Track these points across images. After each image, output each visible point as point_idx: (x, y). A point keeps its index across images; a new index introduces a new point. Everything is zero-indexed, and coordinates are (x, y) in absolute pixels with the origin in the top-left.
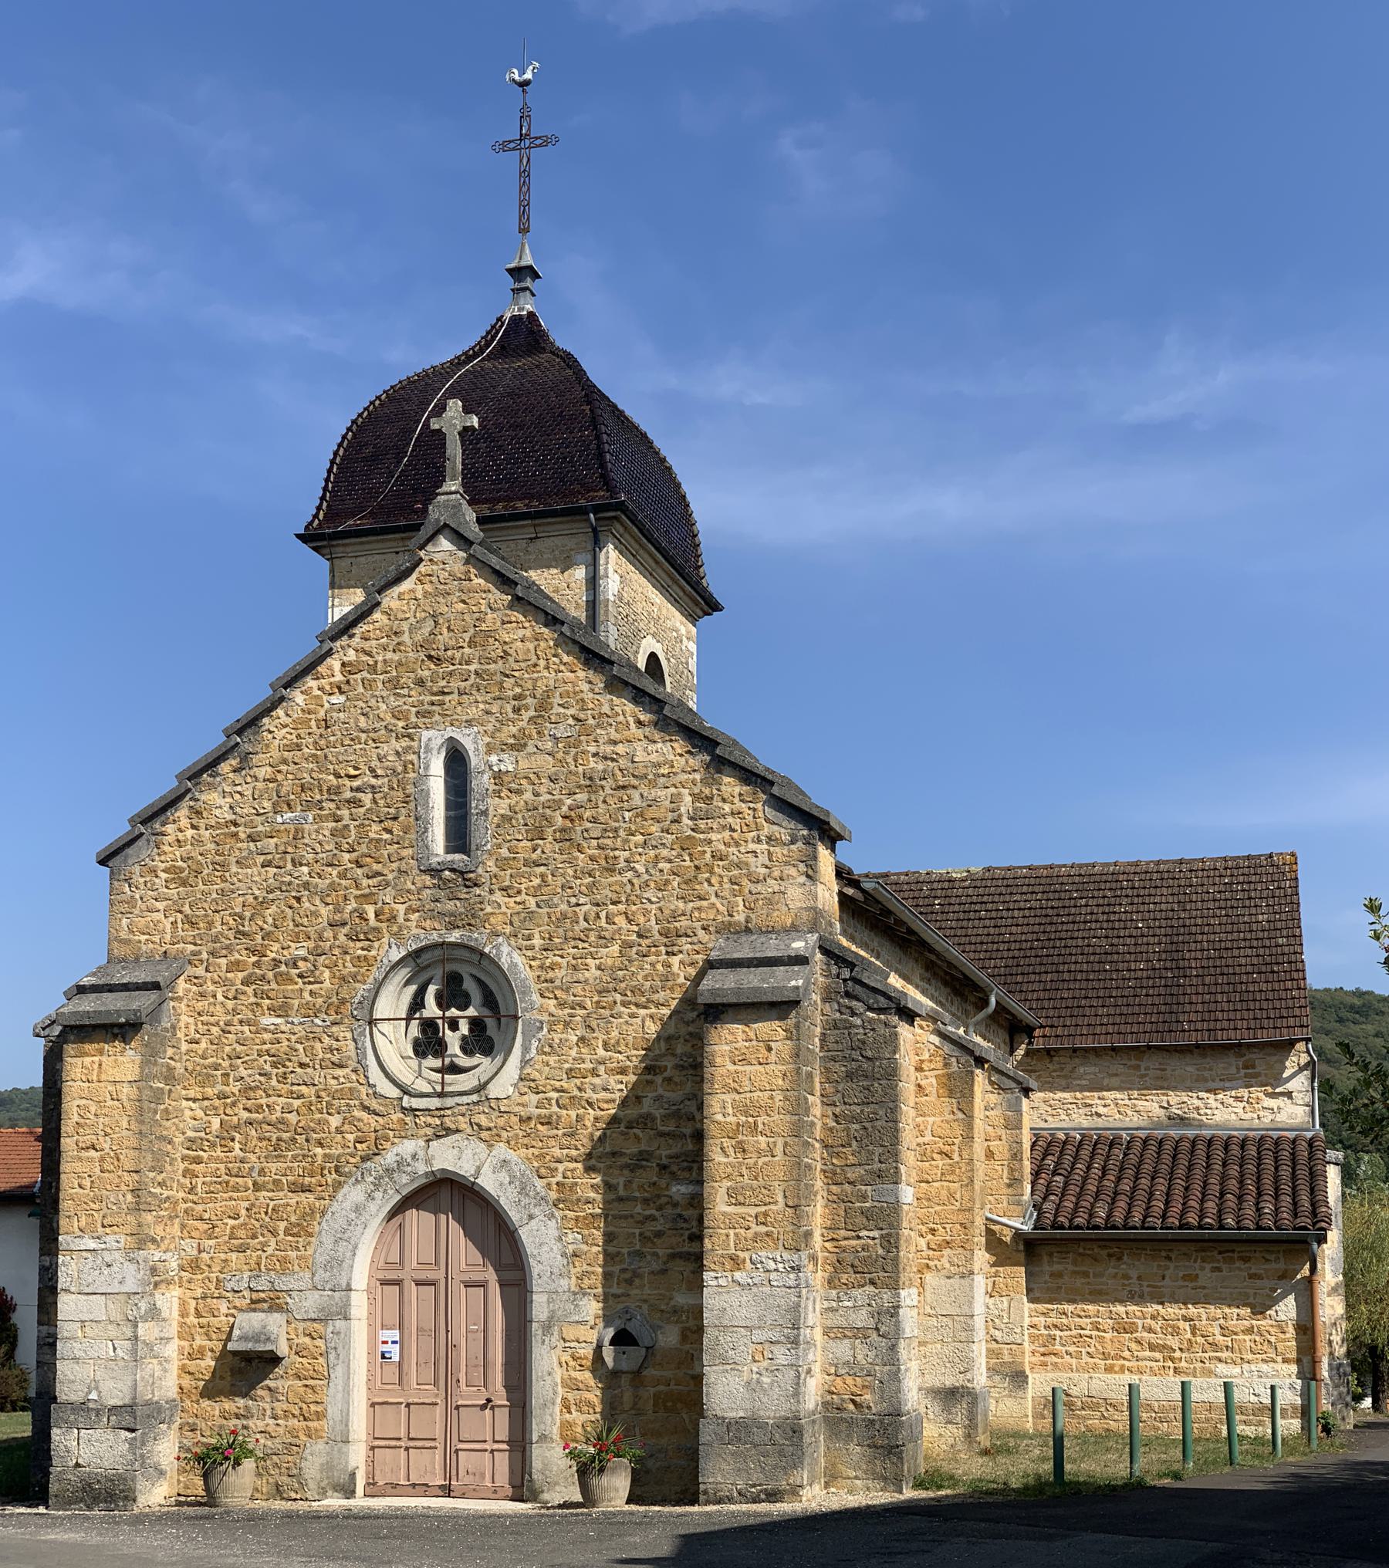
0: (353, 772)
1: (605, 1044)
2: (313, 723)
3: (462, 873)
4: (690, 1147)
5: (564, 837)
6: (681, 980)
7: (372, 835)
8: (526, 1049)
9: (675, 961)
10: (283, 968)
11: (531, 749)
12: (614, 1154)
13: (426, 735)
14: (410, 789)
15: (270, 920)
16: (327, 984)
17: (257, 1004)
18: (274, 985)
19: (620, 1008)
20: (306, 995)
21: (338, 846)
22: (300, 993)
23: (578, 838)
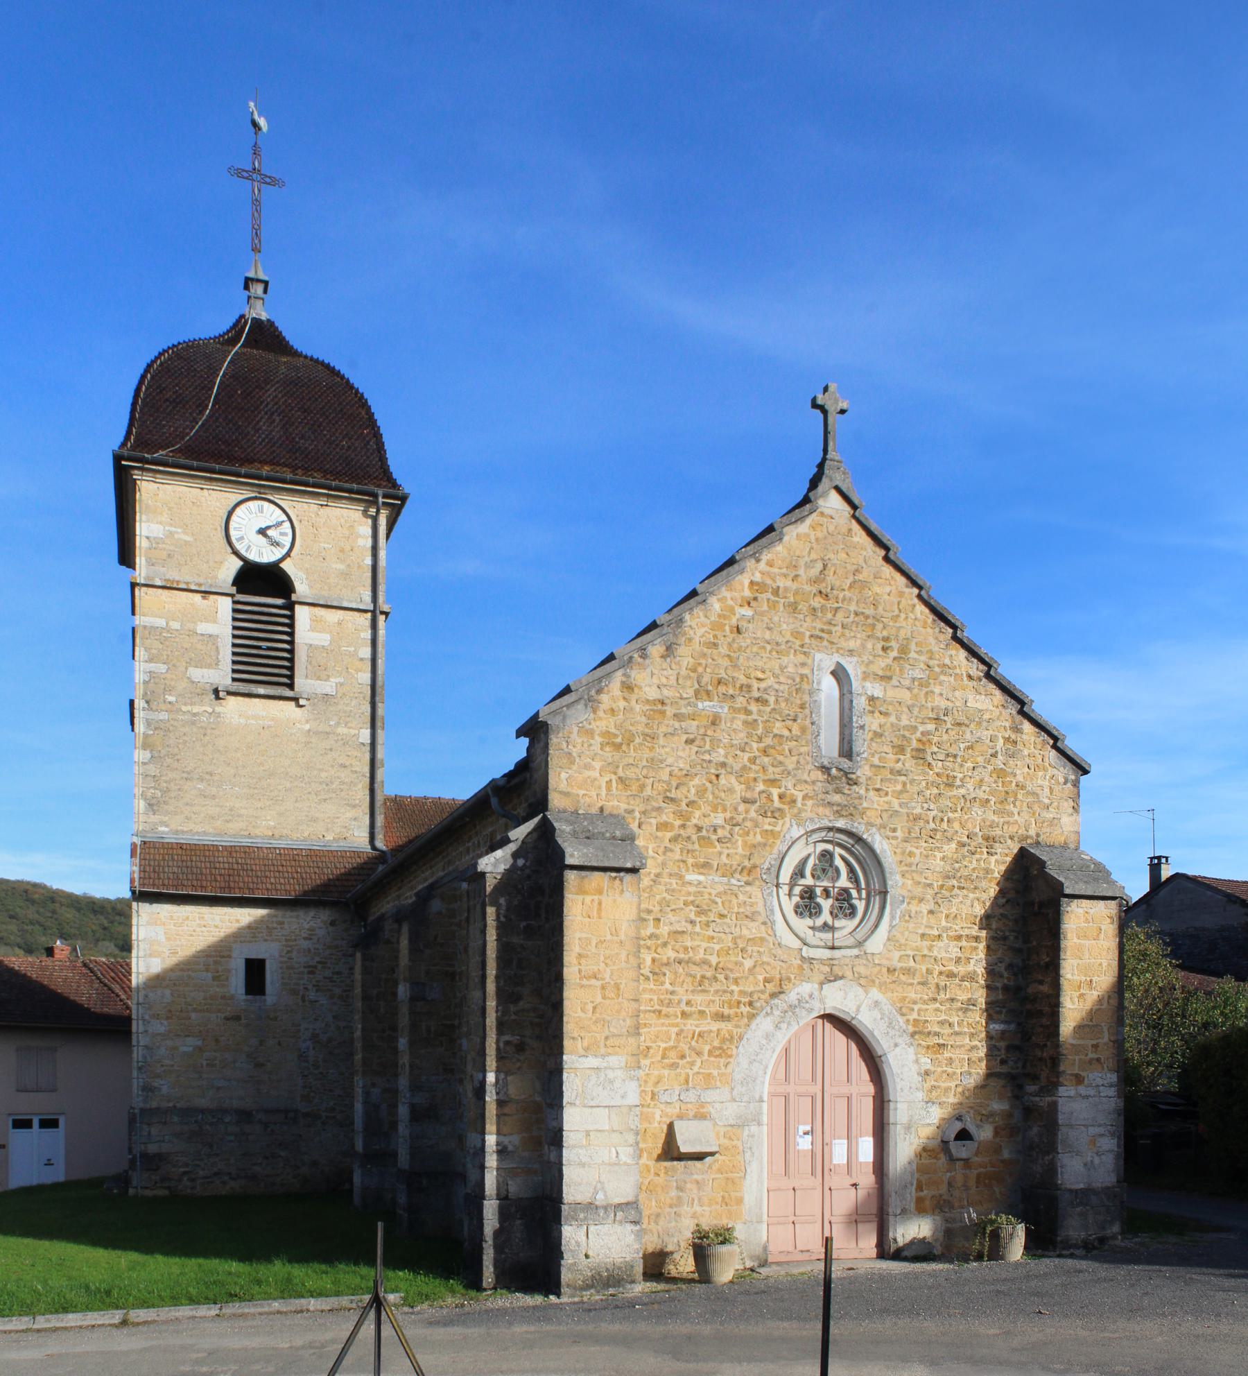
0: (760, 675)
1: (947, 916)
2: (727, 628)
3: (846, 774)
5: (919, 754)
6: (996, 875)
7: (776, 731)
8: (893, 917)
9: (993, 859)
10: (704, 833)
11: (894, 682)
12: (952, 1000)
13: (818, 656)
14: (806, 698)
15: (693, 791)
16: (740, 850)
17: (684, 861)
18: (696, 846)
20: (724, 857)
21: (749, 735)
23: (929, 759)
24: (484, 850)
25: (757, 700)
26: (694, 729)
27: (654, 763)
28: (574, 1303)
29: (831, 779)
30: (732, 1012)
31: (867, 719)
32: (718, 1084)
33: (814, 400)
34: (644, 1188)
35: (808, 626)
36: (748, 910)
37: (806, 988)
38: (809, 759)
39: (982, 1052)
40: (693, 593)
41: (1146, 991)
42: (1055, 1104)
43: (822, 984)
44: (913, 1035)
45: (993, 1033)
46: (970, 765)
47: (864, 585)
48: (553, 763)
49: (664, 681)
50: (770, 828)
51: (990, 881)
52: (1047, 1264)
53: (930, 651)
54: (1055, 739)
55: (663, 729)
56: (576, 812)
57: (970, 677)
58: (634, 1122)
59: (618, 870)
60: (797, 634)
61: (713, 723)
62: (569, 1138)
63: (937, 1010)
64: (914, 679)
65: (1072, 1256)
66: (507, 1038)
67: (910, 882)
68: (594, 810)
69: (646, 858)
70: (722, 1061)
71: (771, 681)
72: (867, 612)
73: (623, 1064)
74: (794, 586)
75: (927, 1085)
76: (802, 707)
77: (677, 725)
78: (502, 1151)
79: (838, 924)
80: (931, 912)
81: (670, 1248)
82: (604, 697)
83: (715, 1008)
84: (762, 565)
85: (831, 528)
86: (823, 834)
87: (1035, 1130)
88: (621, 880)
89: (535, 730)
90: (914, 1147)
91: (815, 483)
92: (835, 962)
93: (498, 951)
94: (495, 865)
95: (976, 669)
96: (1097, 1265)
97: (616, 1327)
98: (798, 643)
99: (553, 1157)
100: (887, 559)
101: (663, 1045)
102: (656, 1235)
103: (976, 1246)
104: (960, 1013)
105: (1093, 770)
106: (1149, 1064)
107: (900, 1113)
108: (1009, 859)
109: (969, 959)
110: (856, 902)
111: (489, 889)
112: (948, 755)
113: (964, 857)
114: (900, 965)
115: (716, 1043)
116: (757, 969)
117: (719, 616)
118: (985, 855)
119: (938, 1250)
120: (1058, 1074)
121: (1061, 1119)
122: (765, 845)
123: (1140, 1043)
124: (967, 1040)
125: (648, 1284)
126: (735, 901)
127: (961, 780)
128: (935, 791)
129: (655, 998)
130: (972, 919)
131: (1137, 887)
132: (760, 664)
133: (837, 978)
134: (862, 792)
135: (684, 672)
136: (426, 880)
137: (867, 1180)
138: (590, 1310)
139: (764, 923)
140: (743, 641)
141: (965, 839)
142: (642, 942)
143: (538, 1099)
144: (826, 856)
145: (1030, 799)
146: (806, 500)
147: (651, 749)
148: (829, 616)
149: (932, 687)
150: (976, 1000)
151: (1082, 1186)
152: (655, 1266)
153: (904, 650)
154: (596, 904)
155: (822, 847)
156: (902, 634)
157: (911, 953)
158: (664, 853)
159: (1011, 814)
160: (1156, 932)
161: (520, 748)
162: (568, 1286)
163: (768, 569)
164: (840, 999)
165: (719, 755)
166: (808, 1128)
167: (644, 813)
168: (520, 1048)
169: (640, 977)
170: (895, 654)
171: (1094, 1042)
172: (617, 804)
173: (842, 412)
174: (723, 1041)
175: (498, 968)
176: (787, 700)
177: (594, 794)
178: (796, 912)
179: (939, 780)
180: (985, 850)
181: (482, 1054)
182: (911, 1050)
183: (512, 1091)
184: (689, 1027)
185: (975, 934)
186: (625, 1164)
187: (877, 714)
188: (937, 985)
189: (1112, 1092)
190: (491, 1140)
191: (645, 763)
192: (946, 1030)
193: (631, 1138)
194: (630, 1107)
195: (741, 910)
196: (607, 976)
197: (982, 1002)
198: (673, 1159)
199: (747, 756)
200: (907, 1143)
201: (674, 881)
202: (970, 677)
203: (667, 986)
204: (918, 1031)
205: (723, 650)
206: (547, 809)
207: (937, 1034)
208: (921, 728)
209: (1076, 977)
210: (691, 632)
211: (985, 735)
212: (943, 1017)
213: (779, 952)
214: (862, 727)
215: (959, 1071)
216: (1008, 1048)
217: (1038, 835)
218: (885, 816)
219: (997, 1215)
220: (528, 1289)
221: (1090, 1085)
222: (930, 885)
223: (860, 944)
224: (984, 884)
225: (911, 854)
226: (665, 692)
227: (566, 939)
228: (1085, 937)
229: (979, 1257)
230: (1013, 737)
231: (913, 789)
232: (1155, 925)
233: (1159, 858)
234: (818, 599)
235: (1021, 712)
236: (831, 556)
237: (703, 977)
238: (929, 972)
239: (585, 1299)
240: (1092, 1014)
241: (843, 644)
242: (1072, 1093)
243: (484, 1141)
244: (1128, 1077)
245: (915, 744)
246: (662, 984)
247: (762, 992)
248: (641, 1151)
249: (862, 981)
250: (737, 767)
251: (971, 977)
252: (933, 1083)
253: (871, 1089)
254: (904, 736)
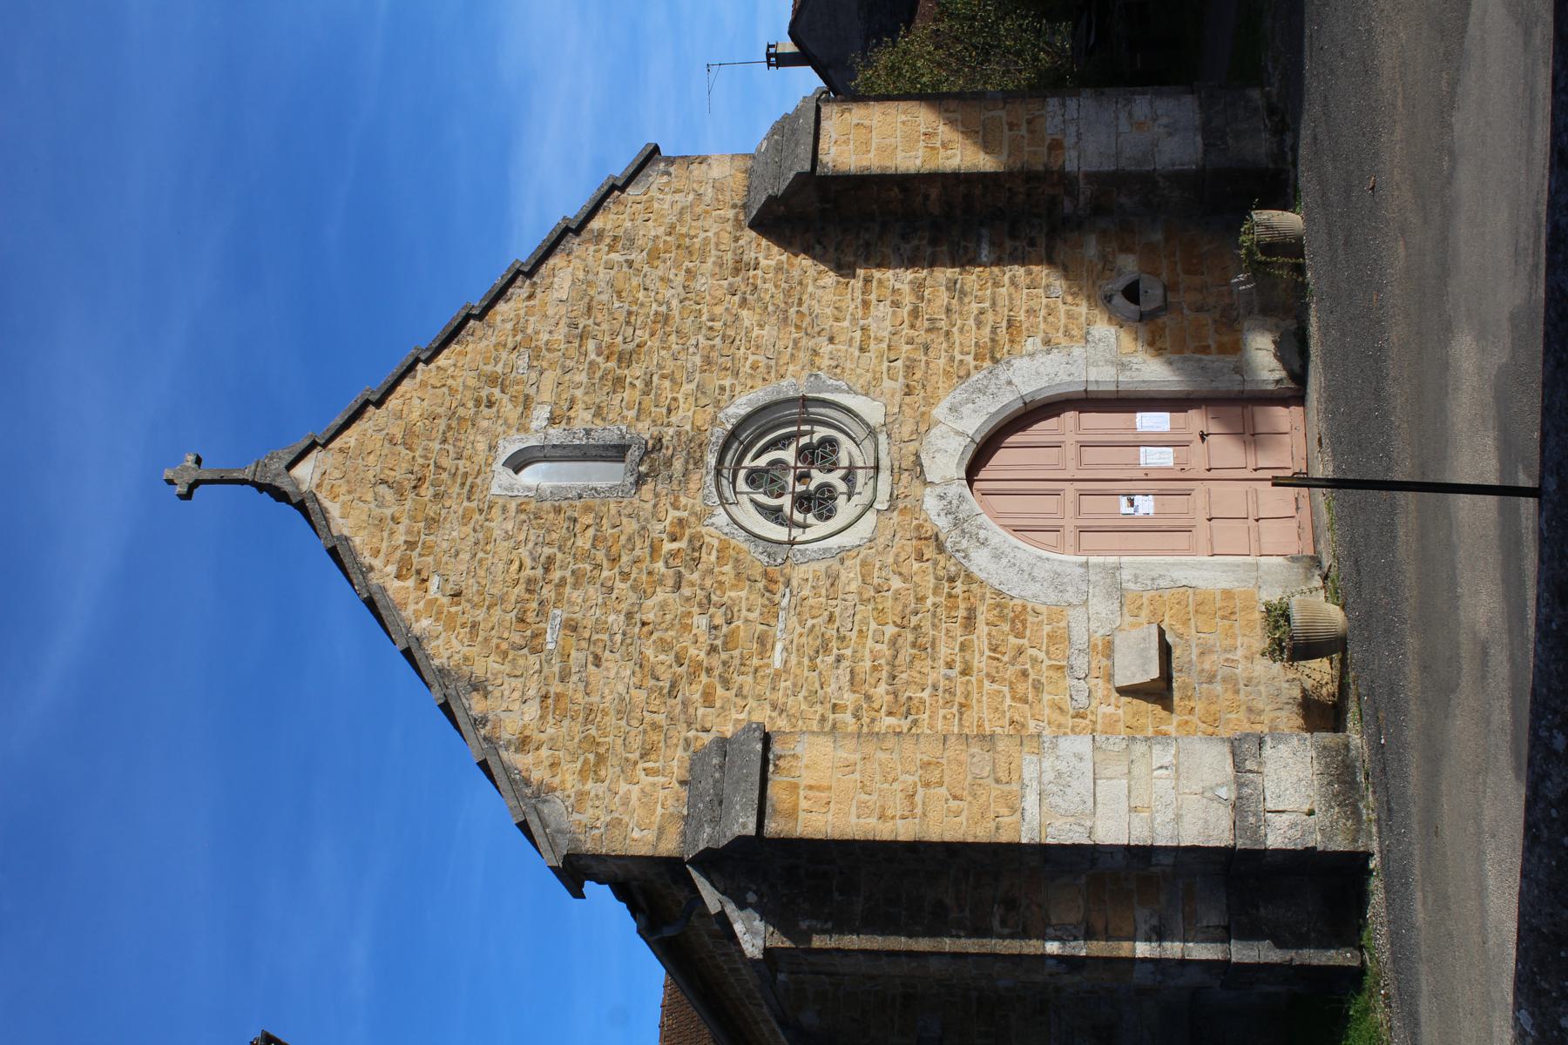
0: (516, 566)
1: (837, 319)
2: (453, 609)
3: (647, 453)
4: (945, 248)
5: (625, 359)
6: (784, 258)
7: (588, 546)
8: (838, 389)
9: (763, 263)
10: (718, 642)
11: (532, 391)
12: (948, 310)
13: (495, 490)
14: (547, 505)
15: (662, 657)
16: (743, 594)
17: (756, 671)
18: (736, 653)
19: (804, 309)
20: (752, 616)
21: (592, 581)
22: (748, 622)
23: (631, 346)
24: (734, 948)
25: (547, 570)
26: (581, 655)
28: (1380, 832)
29: (653, 473)
30: (962, 606)
31: (578, 425)
32: (1063, 624)
33: (183, 497)
34: (1211, 730)
35: (456, 503)
36: (824, 583)
37: (931, 504)
38: (626, 501)
39: (1019, 271)
40: (407, 654)
41: (939, 65)
42: (1088, 175)
43: (926, 483)
44: (995, 361)
45: (993, 257)
46: (641, 295)
47: (409, 432)
48: (619, 848)
49: (516, 695)
50: (714, 553)
51: (792, 265)
52: (1306, 180)
53: (496, 346)
54: (613, 188)
55: (579, 697)
56: (686, 819)
57: (531, 297)
58: (1117, 744)
59: (765, 762)
60: (466, 518)
61: (574, 629)
62: (1139, 835)
63: (961, 330)
64: (530, 367)
65: (1294, 149)
66: (996, 923)
67: (791, 368)
68: (684, 793)
69: (750, 723)
70: (1030, 619)
71: (524, 552)
72: (442, 428)
73: (1035, 758)
74: (405, 521)
75: (1064, 342)
76: (558, 510)
77: (575, 678)
78: (1159, 934)
79: (845, 462)
80: (831, 340)
81: (1297, 693)
82: (536, 776)
83: (957, 630)
84: (377, 563)
85: (337, 474)
86: (724, 482)
87: (1123, 200)
88: (779, 757)
89: (575, 871)
90: (1147, 357)
91: (280, 495)
92: (896, 464)
93: (873, 933)
94: (755, 934)
95: (520, 290)
96: (1305, 117)
97: (1414, 773)
98: (476, 516)
99: (1168, 860)
100: (379, 404)
101: (1008, 701)
102: (1278, 713)
103: (1284, 273)
104: (966, 300)
105: (653, 141)
106: (1036, 59)
107: (1102, 377)
108: (764, 242)
109: (894, 291)
110: (816, 438)
111: (788, 944)
112: (628, 323)
113: (760, 299)
114: (901, 379)
115: (1006, 627)
116: (904, 571)
117: (437, 620)
118: (759, 272)
119: (1291, 324)
120: (1048, 172)
121: (1108, 166)
122: (737, 560)
123: (1008, 71)
124: (1003, 290)
125: (1350, 725)
126: (811, 601)
127: (660, 305)
128: (673, 338)
129: (942, 712)
130: (841, 287)
131: (807, 80)
132: (501, 566)
133: (918, 462)
134: (671, 431)
135: (507, 668)
136: (773, 1031)
137: (1195, 420)
138: (1390, 810)
139: (842, 561)
140: (471, 590)
141: (736, 298)
142: (865, 730)
143: (1083, 880)
144: (754, 478)
145: (687, 217)
146: (301, 507)
147: (605, 713)
148: (444, 476)
149: (541, 343)
150: (949, 280)
151: (1199, 139)
152: (1321, 714)
153: (493, 380)
154: (811, 794)
155: (741, 484)
156: (472, 382)
157: (886, 364)
158: (745, 697)
159: (706, 241)
160: (864, 53)
161: (599, 894)
162: (1355, 840)
163: (382, 554)
164: (945, 460)
165: (615, 620)
166: (1124, 500)
167: (689, 725)
168: (1010, 904)
169: (912, 734)
170: (497, 391)
171: (1006, 127)
172: (676, 761)
173: (198, 461)
174: (1002, 617)
175: (897, 933)
176: (549, 531)
177: (661, 794)
178: (828, 518)
179: (660, 333)
180: (751, 273)
181: (1020, 958)
182: (1016, 363)
183: (1073, 917)
184: (983, 665)
185: (860, 284)
186: (1176, 756)
187: (572, 413)
188: (929, 330)
189: (1072, 104)
190: (1143, 949)
191: (623, 723)
192: (989, 317)
193: (1139, 748)
194: (1096, 749)
195: (823, 592)
196: (910, 779)
197: (951, 273)
198: (1169, 688)
199: (619, 585)
200: (1144, 367)
201: (783, 685)
202: (531, 297)
203: (925, 695)
204: (991, 354)
205: (480, 615)
206: (681, 859)
207: (994, 330)
208: (593, 356)
209: (920, 153)
210: (456, 657)
211: (604, 275)
212: (971, 322)
213: (881, 541)
214: (588, 432)
215: (1044, 301)
216: (1013, 236)
217: (734, 206)
218: (703, 401)
219: (1240, 247)
220: (1362, 899)
221: (1063, 131)
222: (796, 342)
223: (872, 432)
224: (796, 273)
225: (754, 367)
226: (531, 693)
227: (859, 836)
228: (867, 143)
229: (1300, 269)
230: (608, 241)
231: (670, 365)
232: (855, 57)
233: (769, 56)
234: (423, 491)
235: (577, 231)
236: (371, 473)
237: (914, 645)
239: (1373, 816)
240: (968, 131)
241: (480, 458)
242: (1074, 154)
243: (1144, 960)
244: (1052, 84)
245: (612, 364)
246: (922, 702)
247: (936, 563)
248: (1158, 732)
249: (923, 429)
250: (633, 597)
251: (918, 287)
252: (1060, 334)
253: (1069, 417)
254: (601, 378)
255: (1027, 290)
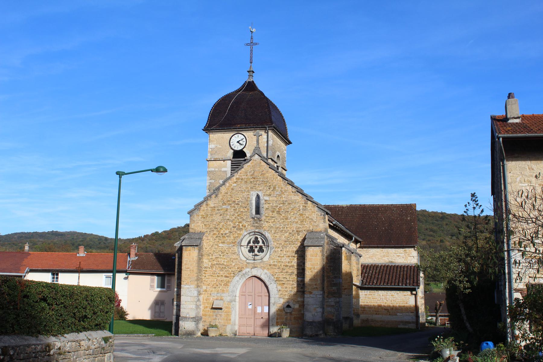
5: (278, 212)
8: (270, 252)
13: (252, 192)
27: (213, 221)
31: (264, 205)
35: (249, 186)
36: (234, 252)
37: (247, 270)
39: (296, 285)
60: (247, 188)
82: (202, 208)
153: (274, 188)
192: (286, 280)
204: (277, 280)
223: (262, 259)
224: (296, 243)
238: (281, 265)
241: (258, 189)
245: (277, 210)
251: (293, 266)
255: (291, 287)
